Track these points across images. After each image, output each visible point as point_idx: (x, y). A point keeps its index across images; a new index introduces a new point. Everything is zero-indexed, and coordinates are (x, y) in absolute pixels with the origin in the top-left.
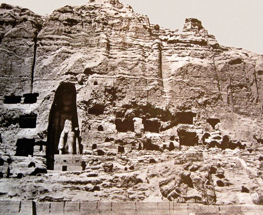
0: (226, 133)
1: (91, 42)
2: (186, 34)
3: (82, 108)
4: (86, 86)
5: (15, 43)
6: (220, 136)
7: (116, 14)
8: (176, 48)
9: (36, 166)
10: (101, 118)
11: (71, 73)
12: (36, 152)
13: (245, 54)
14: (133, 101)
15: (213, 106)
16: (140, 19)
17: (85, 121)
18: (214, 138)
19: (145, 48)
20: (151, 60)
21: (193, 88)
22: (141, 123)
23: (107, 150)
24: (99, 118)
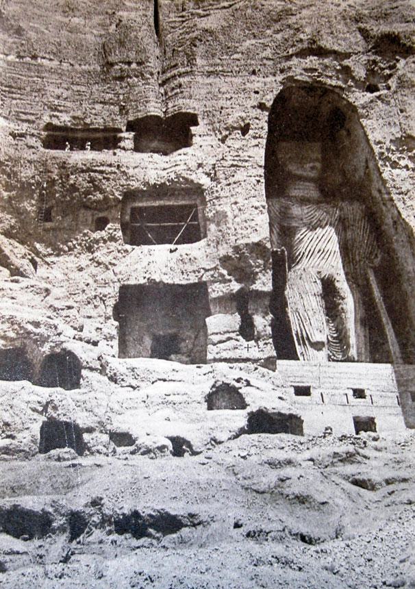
9: (248, 400)
11: (321, 52)
12: (220, 342)
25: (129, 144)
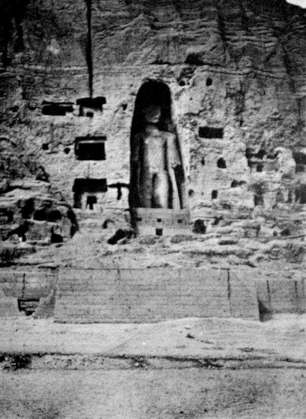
14: (274, 117)
17: (196, 148)
23: (236, 202)
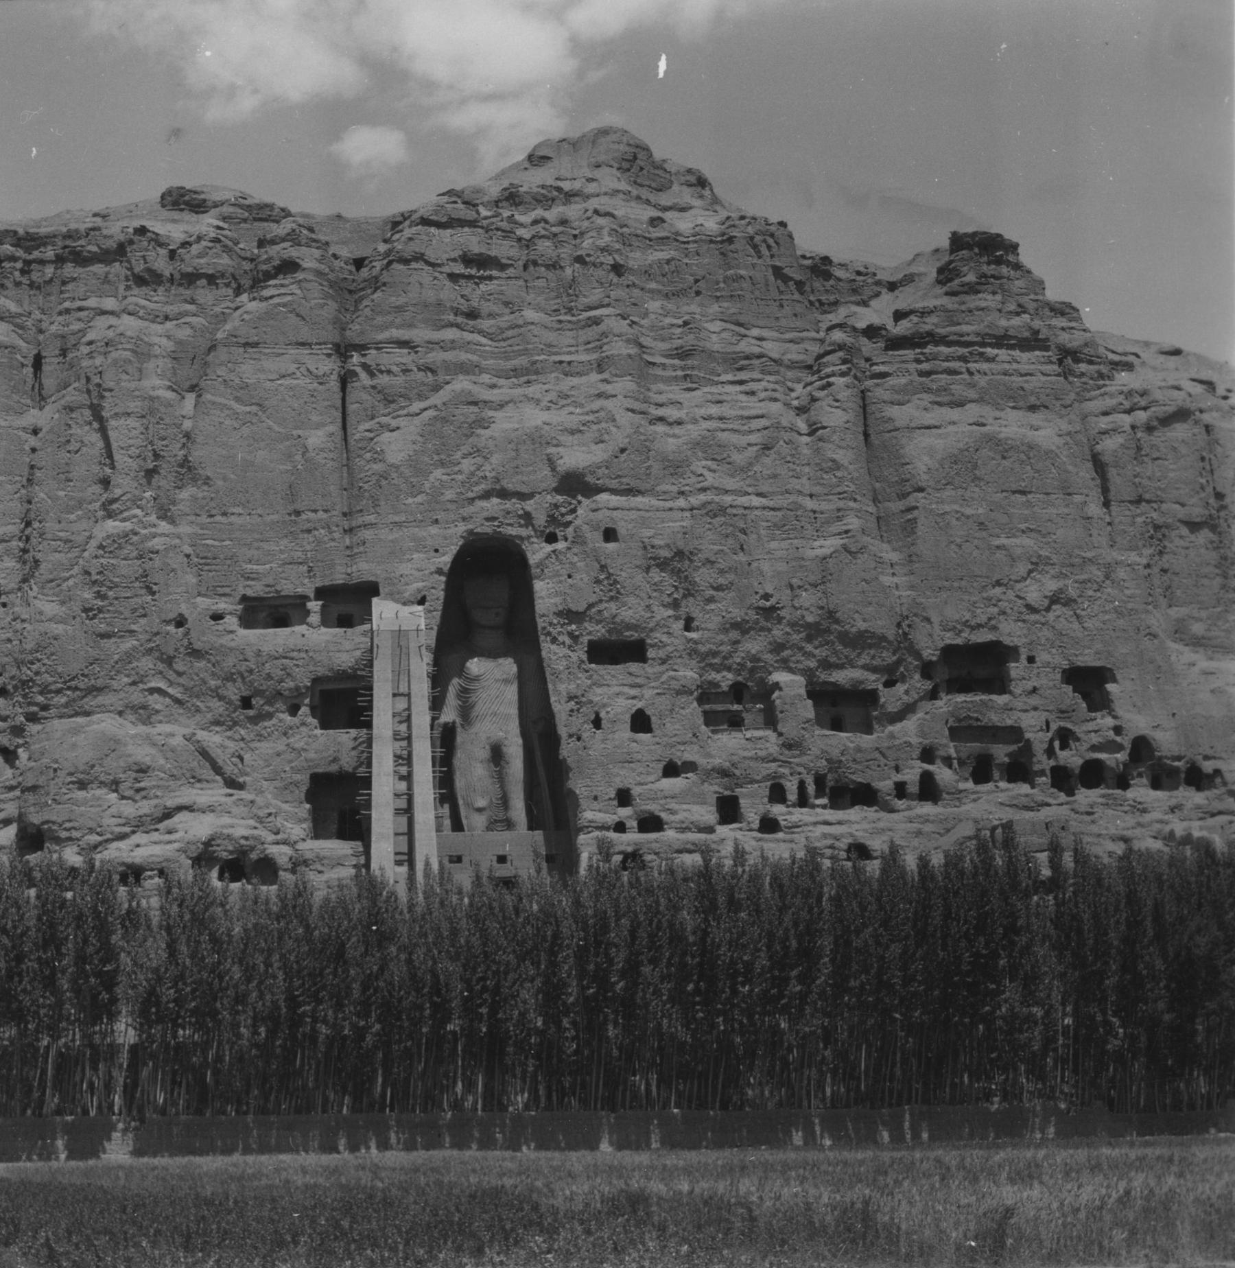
0: (1138, 723)
1: (570, 353)
2: (964, 303)
3: (561, 639)
4: (569, 548)
5: (262, 371)
6: (1118, 739)
7: (655, 222)
8: (925, 366)
10: (638, 681)
11: (504, 494)
13: (1201, 382)
14: (763, 603)
15: (1083, 613)
16: (758, 239)
17: (579, 694)
18: (1094, 748)
19: (788, 367)
20: (824, 428)
21: (1003, 541)
22: (800, 695)
24: (630, 680)
25: (314, 618)
